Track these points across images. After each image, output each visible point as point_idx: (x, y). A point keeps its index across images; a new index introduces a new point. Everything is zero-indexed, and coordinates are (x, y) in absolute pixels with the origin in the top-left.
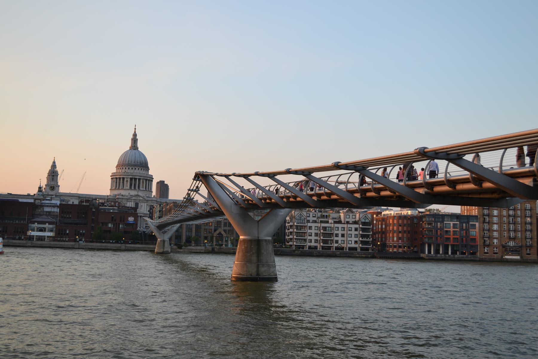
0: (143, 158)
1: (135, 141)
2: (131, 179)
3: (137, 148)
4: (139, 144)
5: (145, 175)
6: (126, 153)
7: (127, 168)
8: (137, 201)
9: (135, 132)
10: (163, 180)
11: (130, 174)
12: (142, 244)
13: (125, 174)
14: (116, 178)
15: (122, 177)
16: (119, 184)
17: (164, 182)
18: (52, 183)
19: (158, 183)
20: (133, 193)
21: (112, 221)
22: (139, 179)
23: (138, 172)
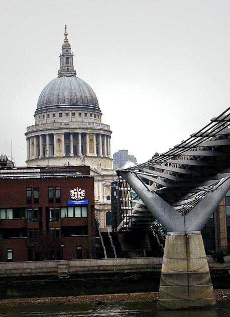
0: (87, 92)
1: (67, 59)
2: (67, 136)
3: (72, 74)
4: (77, 65)
5: (94, 126)
6: (51, 86)
7: (57, 115)
9: (66, 41)
11: (63, 126)
12: (111, 256)
13: (55, 126)
14: (38, 137)
15: (47, 133)
16: (44, 149)
21: (29, 202)
22: (84, 135)
23: (80, 120)
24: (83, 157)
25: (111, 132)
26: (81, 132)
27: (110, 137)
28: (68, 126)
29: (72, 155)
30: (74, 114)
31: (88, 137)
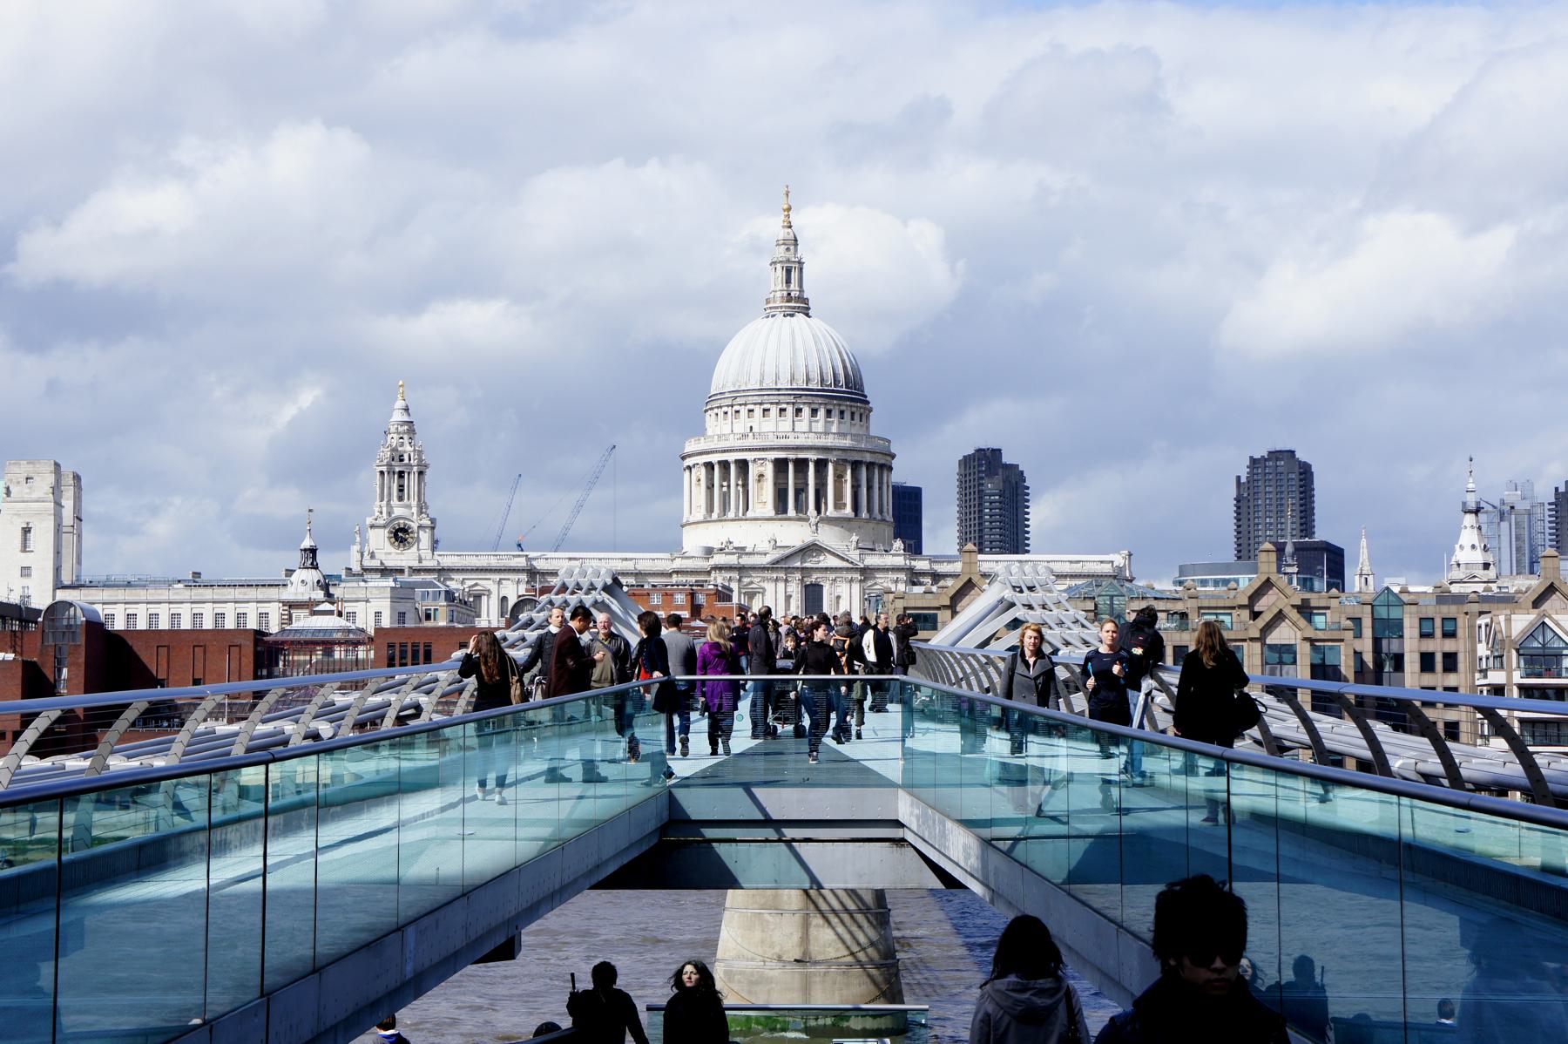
1: (789, 271)
2: (780, 465)
7: (758, 410)
8: (813, 578)
10: (995, 447)
13: (750, 442)
14: (709, 466)
15: (731, 457)
16: (725, 498)
17: (997, 452)
18: (398, 512)
19: (966, 462)
20: (794, 534)
24: (813, 520)
25: (893, 456)
26: (815, 457)
27: (890, 469)
28: (783, 442)
29: (791, 512)
30: (799, 411)
31: (831, 467)
